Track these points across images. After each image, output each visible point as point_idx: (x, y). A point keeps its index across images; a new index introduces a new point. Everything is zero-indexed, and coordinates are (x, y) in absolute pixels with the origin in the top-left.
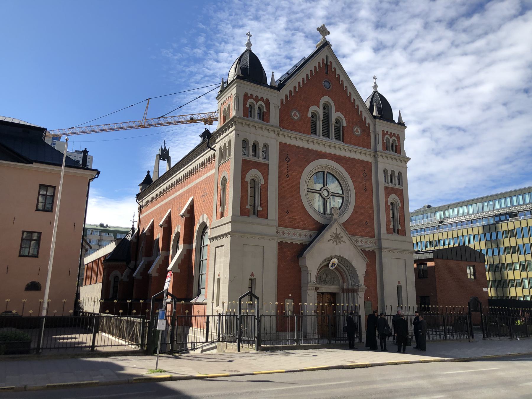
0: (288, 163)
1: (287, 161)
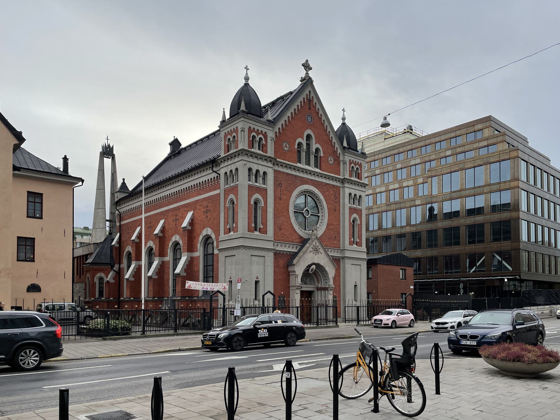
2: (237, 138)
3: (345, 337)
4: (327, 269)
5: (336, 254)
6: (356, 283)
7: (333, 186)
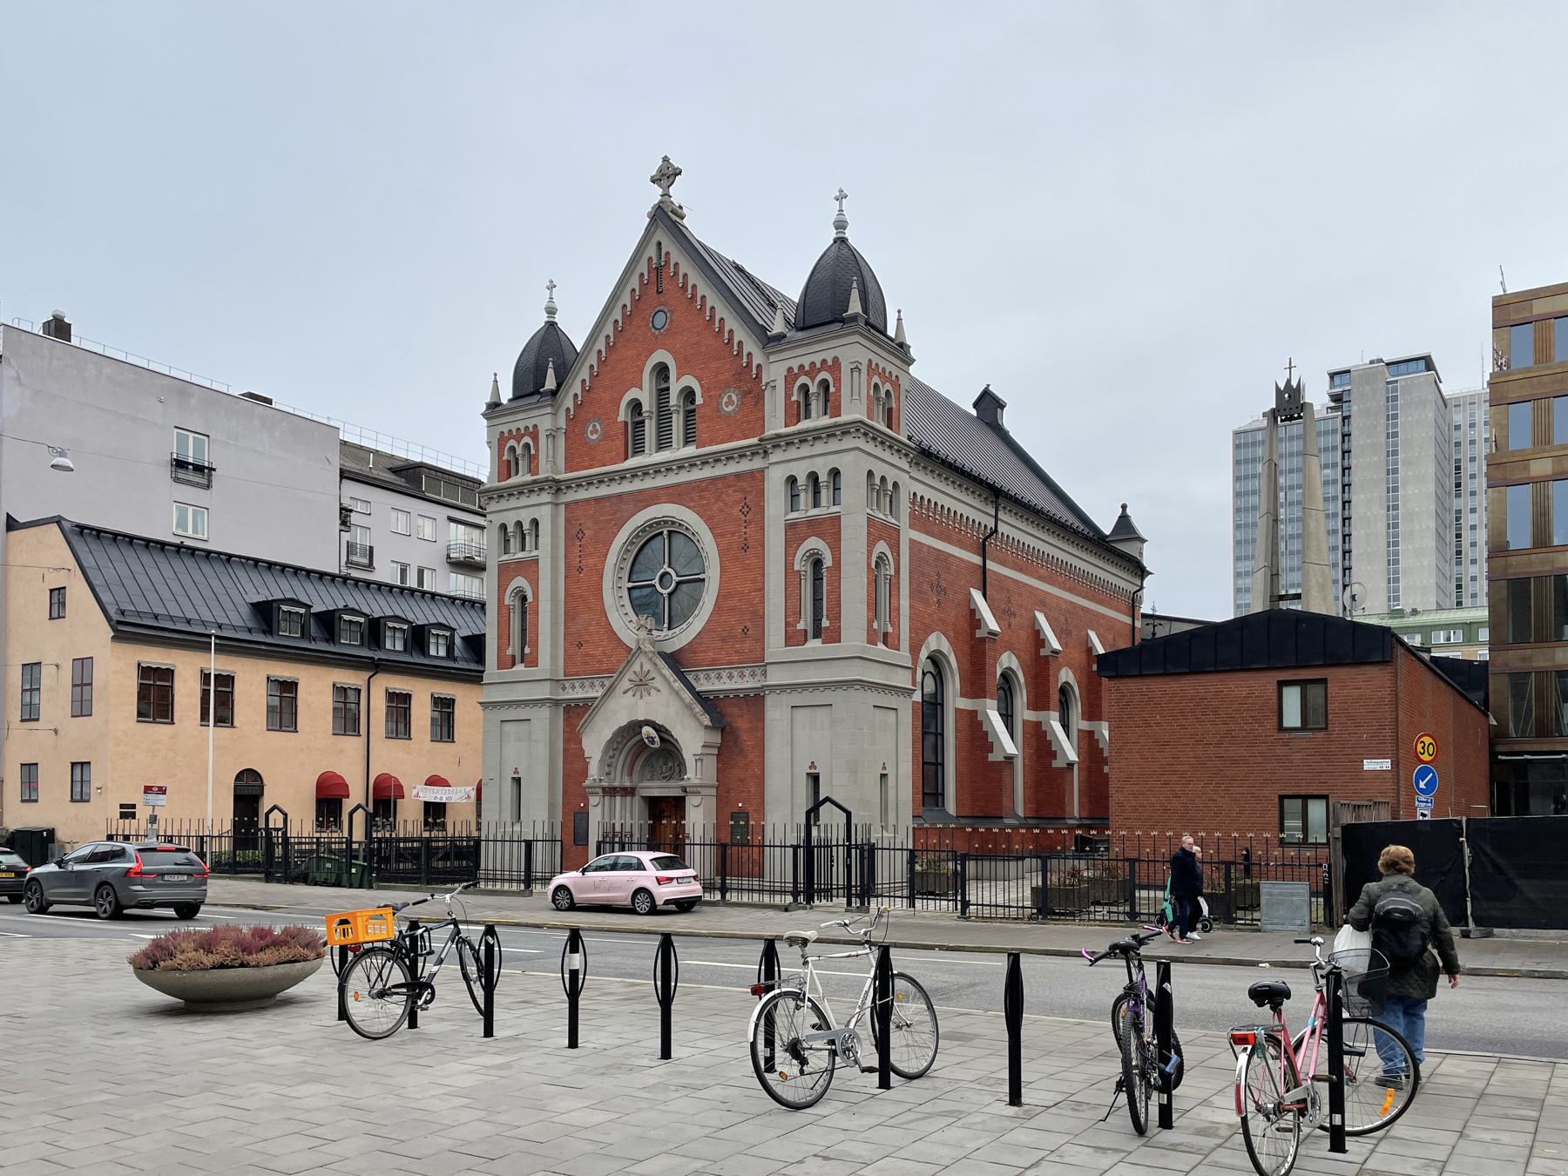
2: (537, 450)
6: (815, 768)
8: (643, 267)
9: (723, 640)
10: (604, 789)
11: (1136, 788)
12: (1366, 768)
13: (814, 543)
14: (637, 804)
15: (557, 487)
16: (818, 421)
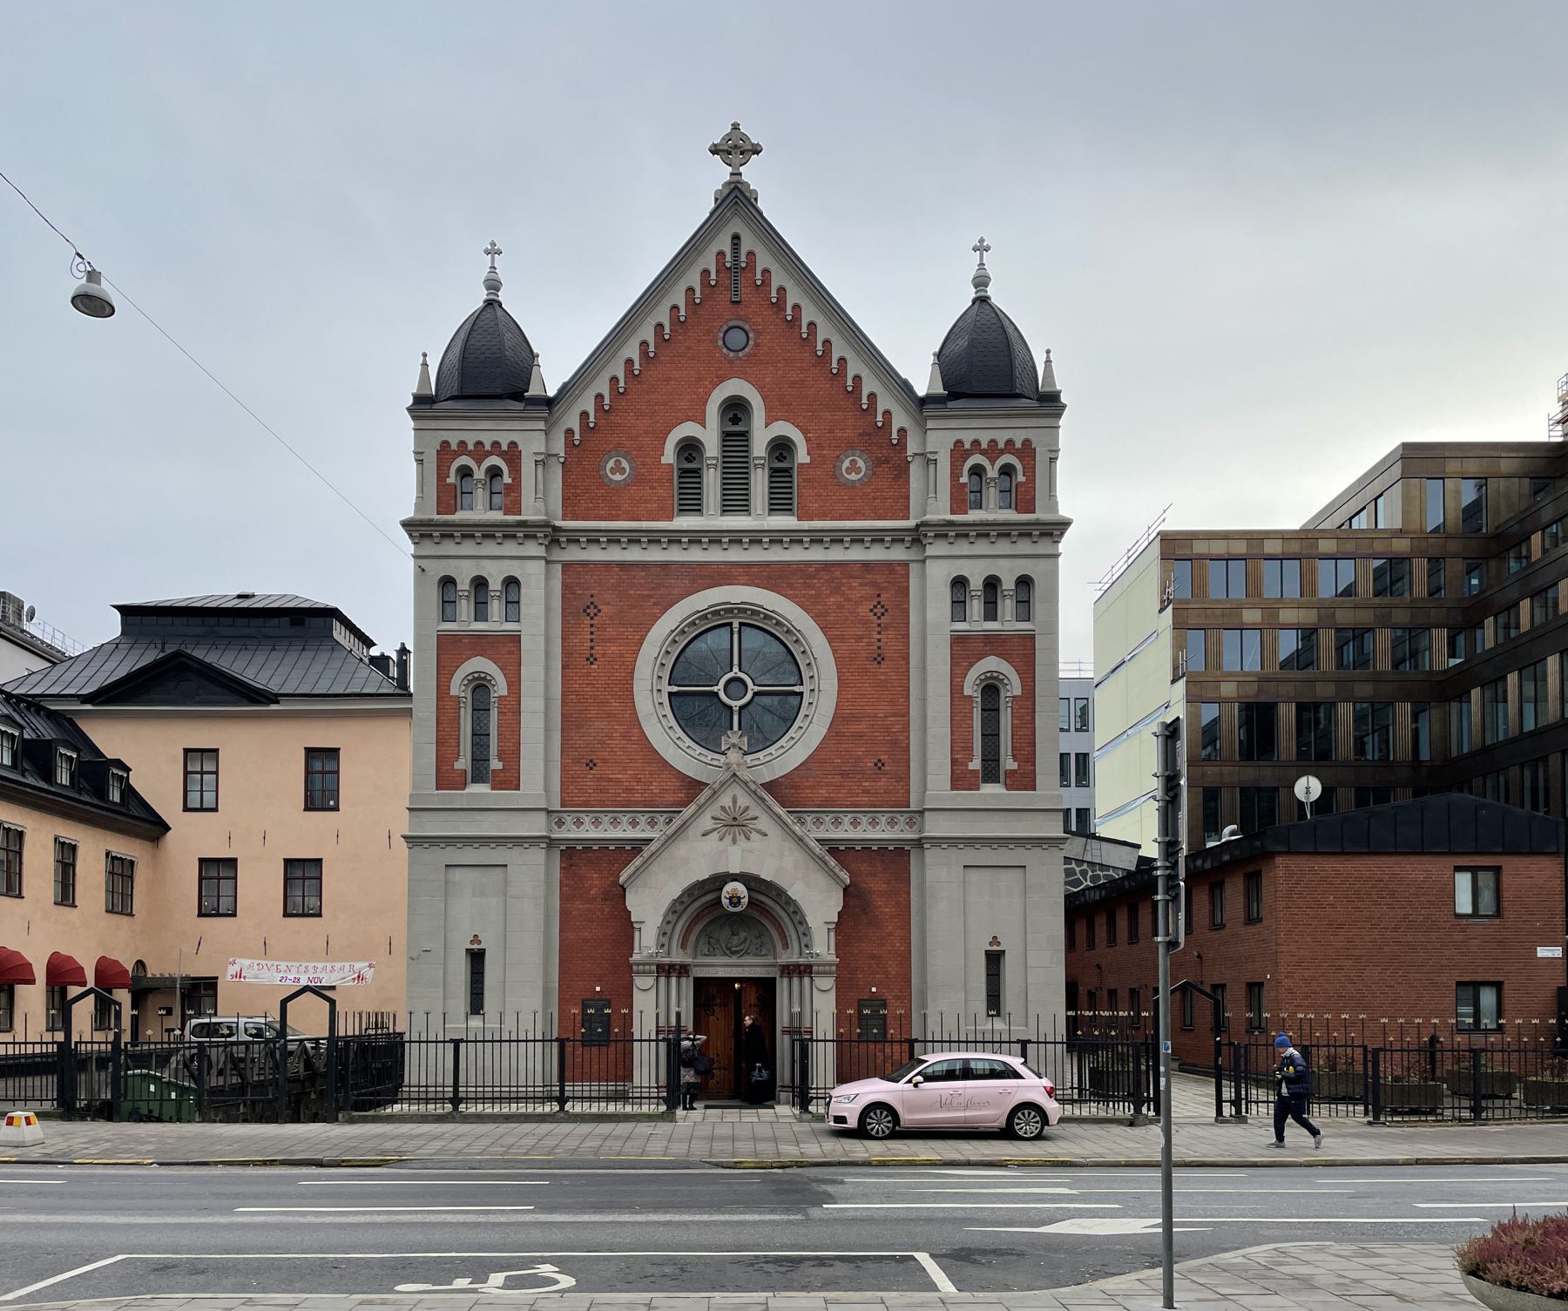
0: (593, 622)
1: (588, 615)
3: (741, 1162)
4: (795, 892)
5: (881, 831)
6: (999, 944)
7: (867, 565)
8: (708, 261)
9: (844, 775)
10: (658, 966)
11: (1307, 974)
12: (1539, 955)
13: (992, 663)
14: (688, 986)
15: (554, 537)
16: (993, 512)
